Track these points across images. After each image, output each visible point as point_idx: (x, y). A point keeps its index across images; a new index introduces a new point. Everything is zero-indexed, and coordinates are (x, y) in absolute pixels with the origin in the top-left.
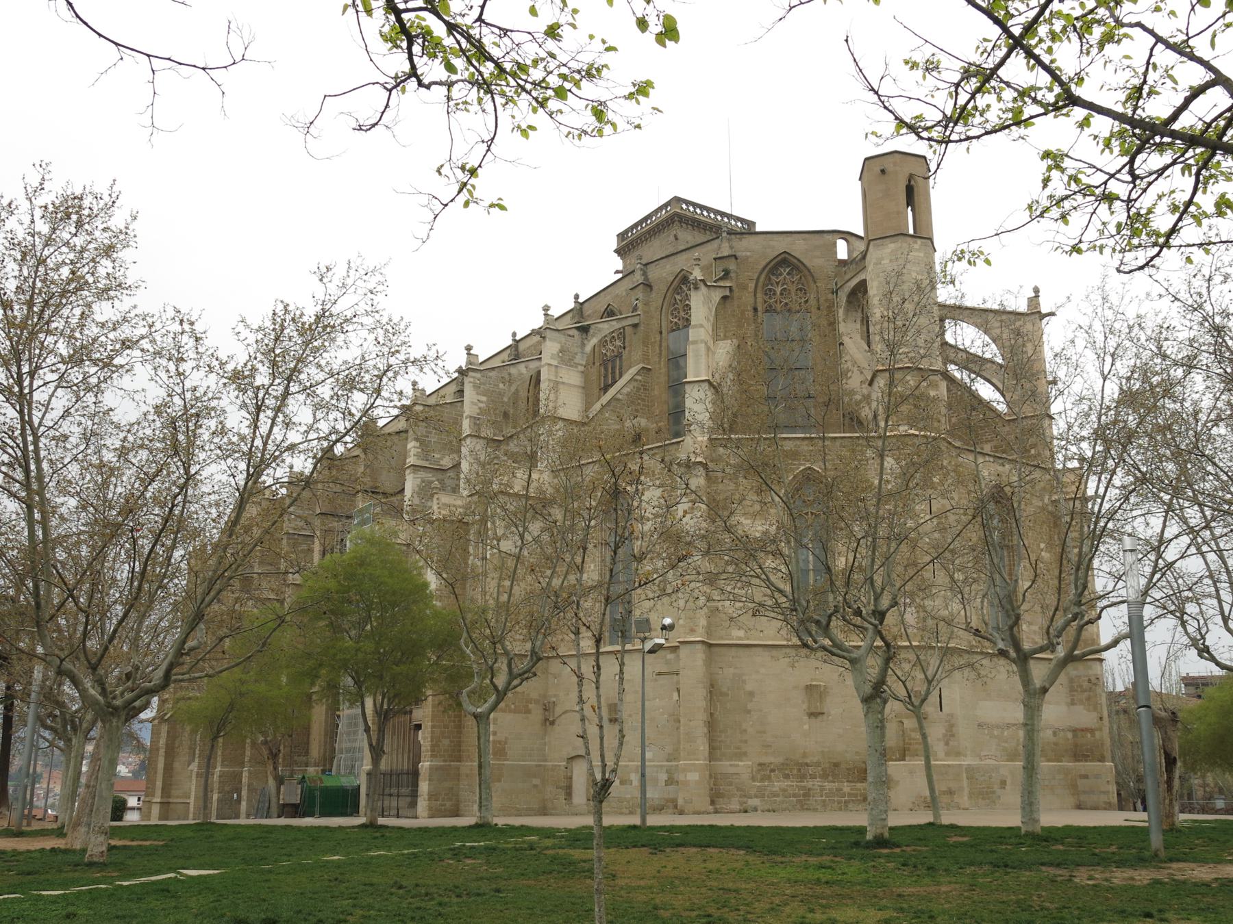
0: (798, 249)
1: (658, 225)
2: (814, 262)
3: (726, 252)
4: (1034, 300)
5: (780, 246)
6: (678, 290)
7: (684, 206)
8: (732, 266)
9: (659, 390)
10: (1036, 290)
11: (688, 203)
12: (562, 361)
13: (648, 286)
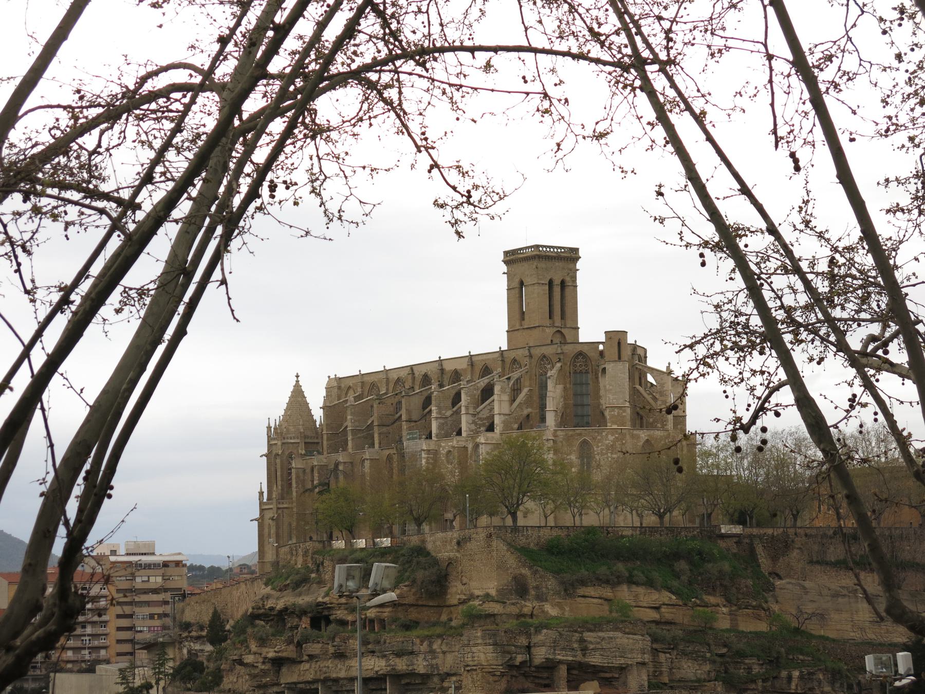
1: (527, 257)
2: (591, 354)
3: (559, 351)
4: (668, 367)
6: (542, 360)
7: (541, 249)
8: (562, 357)
9: (536, 398)
10: (669, 364)
11: (543, 246)
12: (502, 392)
13: (531, 356)
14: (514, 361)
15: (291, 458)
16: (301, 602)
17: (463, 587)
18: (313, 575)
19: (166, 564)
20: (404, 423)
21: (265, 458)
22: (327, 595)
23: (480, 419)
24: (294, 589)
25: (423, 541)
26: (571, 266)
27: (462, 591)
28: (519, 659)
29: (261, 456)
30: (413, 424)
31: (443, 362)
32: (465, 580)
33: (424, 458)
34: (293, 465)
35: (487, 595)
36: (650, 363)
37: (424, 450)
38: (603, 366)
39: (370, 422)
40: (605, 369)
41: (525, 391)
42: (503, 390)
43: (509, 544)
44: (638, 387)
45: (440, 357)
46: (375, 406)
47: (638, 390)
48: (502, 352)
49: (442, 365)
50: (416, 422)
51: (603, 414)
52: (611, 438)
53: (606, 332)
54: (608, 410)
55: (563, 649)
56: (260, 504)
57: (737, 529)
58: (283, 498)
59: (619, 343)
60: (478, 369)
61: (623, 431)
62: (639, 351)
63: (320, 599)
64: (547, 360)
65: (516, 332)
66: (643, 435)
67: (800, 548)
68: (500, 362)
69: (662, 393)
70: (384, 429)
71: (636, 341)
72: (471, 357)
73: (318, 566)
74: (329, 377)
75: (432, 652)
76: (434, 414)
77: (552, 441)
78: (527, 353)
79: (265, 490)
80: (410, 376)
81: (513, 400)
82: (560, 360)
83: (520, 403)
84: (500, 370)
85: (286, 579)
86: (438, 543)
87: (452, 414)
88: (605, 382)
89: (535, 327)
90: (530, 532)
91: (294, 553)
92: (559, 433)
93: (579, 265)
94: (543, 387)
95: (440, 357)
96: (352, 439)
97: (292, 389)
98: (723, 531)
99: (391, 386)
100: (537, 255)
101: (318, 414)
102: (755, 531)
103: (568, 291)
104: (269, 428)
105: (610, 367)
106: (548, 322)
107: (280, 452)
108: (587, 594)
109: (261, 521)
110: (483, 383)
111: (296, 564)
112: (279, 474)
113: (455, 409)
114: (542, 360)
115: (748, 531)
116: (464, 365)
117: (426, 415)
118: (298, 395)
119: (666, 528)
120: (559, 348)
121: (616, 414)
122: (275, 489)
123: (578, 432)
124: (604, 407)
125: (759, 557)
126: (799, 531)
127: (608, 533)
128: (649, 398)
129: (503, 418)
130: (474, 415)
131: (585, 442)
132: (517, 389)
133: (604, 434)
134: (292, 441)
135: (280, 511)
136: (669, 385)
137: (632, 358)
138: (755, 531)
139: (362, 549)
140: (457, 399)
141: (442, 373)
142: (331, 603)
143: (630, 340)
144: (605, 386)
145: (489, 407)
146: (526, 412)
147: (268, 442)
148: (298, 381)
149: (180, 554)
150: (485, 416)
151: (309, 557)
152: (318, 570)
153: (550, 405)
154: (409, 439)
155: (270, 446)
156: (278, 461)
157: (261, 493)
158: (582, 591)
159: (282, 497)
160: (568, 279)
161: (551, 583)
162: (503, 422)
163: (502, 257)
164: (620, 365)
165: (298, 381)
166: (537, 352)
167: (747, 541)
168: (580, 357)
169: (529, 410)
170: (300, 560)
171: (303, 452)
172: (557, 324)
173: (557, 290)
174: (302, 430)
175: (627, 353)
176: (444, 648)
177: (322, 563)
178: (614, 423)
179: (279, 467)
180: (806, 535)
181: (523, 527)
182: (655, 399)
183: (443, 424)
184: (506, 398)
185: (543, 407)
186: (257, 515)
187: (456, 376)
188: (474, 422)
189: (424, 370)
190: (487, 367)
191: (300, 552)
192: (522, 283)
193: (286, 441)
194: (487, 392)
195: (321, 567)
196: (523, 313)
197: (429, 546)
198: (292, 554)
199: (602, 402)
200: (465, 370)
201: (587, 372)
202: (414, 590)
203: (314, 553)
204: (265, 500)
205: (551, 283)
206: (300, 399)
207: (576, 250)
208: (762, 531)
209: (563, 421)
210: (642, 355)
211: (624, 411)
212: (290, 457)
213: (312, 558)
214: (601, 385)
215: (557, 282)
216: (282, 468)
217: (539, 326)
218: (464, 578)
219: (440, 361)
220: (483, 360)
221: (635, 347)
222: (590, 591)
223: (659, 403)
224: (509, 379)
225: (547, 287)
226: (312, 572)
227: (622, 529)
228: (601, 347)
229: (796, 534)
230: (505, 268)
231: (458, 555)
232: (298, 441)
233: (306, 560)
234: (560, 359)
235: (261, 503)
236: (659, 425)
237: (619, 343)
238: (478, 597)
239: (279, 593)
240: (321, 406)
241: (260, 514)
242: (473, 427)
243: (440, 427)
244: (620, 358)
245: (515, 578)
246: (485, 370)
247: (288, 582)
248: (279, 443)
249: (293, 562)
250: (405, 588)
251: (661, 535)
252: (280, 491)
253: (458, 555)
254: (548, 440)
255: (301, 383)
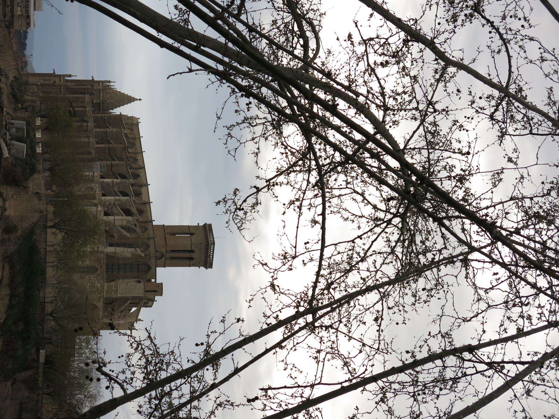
1: (208, 237)
3: (151, 256)
4: (140, 320)
6: (146, 245)
8: (148, 257)
10: (142, 321)
13: (149, 239)
14: (146, 229)
15: (91, 94)
16: (3, 98)
17: (10, 195)
18: (20, 106)
19: (28, 17)
20: (110, 162)
21: (91, 79)
22: (8, 113)
23: (112, 208)
24: (11, 94)
25: (39, 172)
26: (202, 264)
27: (8, 194)
29: (92, 77)
30: (110, 168)
31: (146, 187)
32: (15, 196)
33: (89, 174)
34: (87, 96)
35: (5, 210)
36: (143, 310)
37: (94, 174)
38: (142, 282)
39: (111, 142)
40: (140, 282)
41: (128, 235)
42: (129, 222)
43: (36, 223)
44: (129, 302)
45: (149, 185)
46: (121, 145)
47: (127, 302)
48: (151, 221)
49: (145, 186)
50: (111, 169)
51: (113, 281)
52: (99, 285)
53: (162, 283)
54: (115, 284)
56: (64, 75)
57: (42, 359)
58: (67, 89)
59: (155, 291)
60: (142, 207)
61: (103, 293)
62: (150, 303)
63: (5, 109)
64: (146, 248)
65: (163, 230)
66: (100, 305)
67: (30, 396)
68: (145, 220)
69: (125, 316)
70: (107, 151)
71: (156, 301)
72: (149, 203)
73: (25, 109)
74: (139, 118)
76: (115, 180)
77: (97, 250)
78: (151, 236)
79: (72, 78)
80: (139, 167)
81: (123, 227)
82: (146, 256)
83: (121, 232)
84: (141, 220)
85: (18, 89)
86: (38, 181)
87: (114, 191)
88: (132, 283)
89: (166, 241)
90: (43, 236)
91: (34, 95)
92: (102, 255)
93: (202, 268)
94: (130, 246)
95: (149, 185)
96: (101, 131)
97: (133, 96)
98: (41, 351)
99: (133, 155)
100: (209, 243)
101: (117, 111)
102: (41, 370)
103: (187, 261)
104: (109, 82)
105: (141, 285)
106: (169, 249)
107: (95, 88)
108: (5, 269)
109: (53, 75)
110: (134, 210)
111: (27, 95)
112: (82, 87)
113: (118, 193)
114: (146, 245)
115: (41, 366)
116: (144, 199)
117: (115, 175)
118: (128, 100)
119: (44, 317)
120: (153, 256)
121: (113, 288)
122: (73, 84)
123: (103, 265)
124: (117, 281)
125: (25, 372)
126: (41, 396)
127: (42, 283)
128: (122, 308)
129: (112, 221)
130: (114, 204)
131: (97, 270)
132: (129, 230)
133: (101, 281)
134: (101, 95)
135: (59, 87)
136: (129, 320)
137: (146, 299)
138: (41, 370)
139: (35, 135)
140: (124, 194)
141: (140, 186)
142: (2, 116)
143: (157, 298)
144: (130, 282)
145: (119, 213)
146: (116, 235)
147: (101, 81)
148: (137, 100)
149: (34, 26)
150: (113, 211)
151: (31, 104)
152: (23, 108)
153: (119, 250)
154: (101, 165)
155: (99, 82)
156: (89, 87)
157: (70, 76)
158: (7, 266)
159: (67, 88)
160: (194, 261)
161: (12, 248)
162: (110, 222)
163: (208, 223)
164: (142, 291)
165: (137, 100)
166: (151, 242)
167: (35, 366)
168: (147, 268)
169: (117, 237)
170: (29, 98)
171: (94, 102)
172: (167, 254)
173: (187, 255)
174: (107, 101)
175: (149, 295)
177: (27, 111)
178: (108, 287)
179: (85, 87)
180: (38, 400)
181: (46, 232)
182: (122, 312)
183: (109, 186)
184: (124, 223)
185: (118, 245)
186: (57, 73)
187: (138, 194)
188: (110, 204)
190: (143, 212)
191: (34, 98)
192: (192, 234)
193: (101, 91)
194: (128, 212)
195: (24, 110)
196: (174, 234)
197: (36, 176)
198: (32, 93)
199: (121, 281)
200: (141, 199)
201: (138, 272)
202: (9, 165)
203: (33, 107)
204: (66, 78)
205: (192, 251)
206: (126, 101)
207: (211, 267)
208: (41, 374)
209: (109, 257)
210: (148, 305)
211: (115, 294)
212: (92, 94)
213: (30, 105)
214: (130, 280)
215: (193, 255)
216: (85, 89)
217: (166, 244)
218: (16, 196)
219: (147, 185)
220: (147, 210)
221: (153, 300)
222: (7, 271)
223: (119, 314)
224: (136, 225)
225: (189, 249)
226: (22, 105)
227: (44, 291)
228: (153, 280)
229: (39, 394)
230: (201, 224)
231: (30, 193)
232: (101, 99)
233: (29, 102)
234: (147, 256)
235: (64, 76)
236: (106, 314)
237: (155, 291)
238: (5, 204)
239: (9, 85)
240: (122, 113)
241: (57, 75)
242: (107, 203)
243: (107, 184)
244: (147, 291)
245: (15, 227)
246: (141, 211)
247: (16, 90)
248: (100, 88)
249: (28, 93)
250: (10, 160)
251: (40, 314)
252: (71, 87)
253: (30, 193)
254: (98, 248)
255: (136, 102)
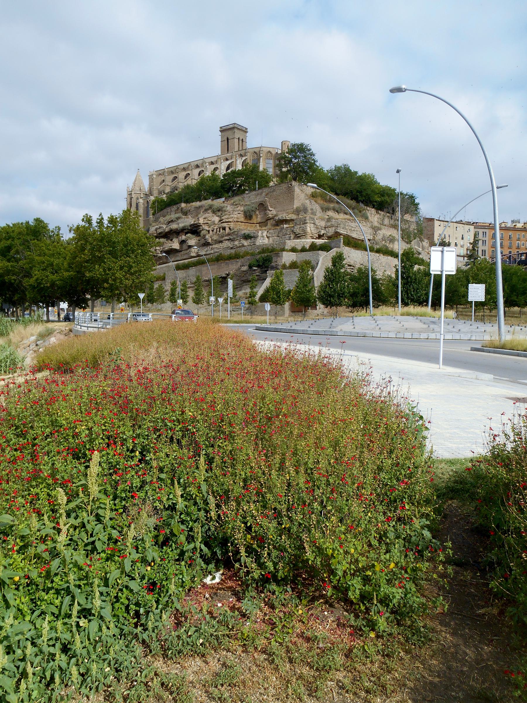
0: (271, 150)
5: (269, 149)
28: (323, 232)
55: (343, 228)
75: (263, 237)
93: (248, 134)
103: (244, 143)
173: (241, 142)
176: (268, 235)
189: (196, 163)
200: (216, 162)
212: (138, 199)
215: (241, 139)
230: (220, 133)
